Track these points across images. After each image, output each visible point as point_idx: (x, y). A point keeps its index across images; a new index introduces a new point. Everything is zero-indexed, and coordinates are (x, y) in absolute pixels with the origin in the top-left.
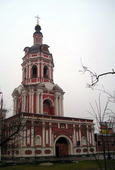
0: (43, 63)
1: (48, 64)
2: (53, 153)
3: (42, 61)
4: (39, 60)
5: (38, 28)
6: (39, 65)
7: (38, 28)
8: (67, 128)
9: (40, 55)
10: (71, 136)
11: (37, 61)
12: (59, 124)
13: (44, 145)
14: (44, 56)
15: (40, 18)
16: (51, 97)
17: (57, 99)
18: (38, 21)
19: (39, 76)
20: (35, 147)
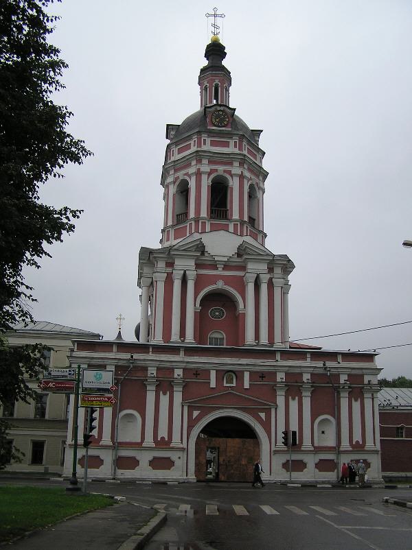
0: (205, 168)
1: (225, 171)
2: (183, 469)
3: (205, 161)
4: (194, 163)
5: (215, 51)
6: (194, 178)
7: (215, 51)
8: (247, 385)
9: (199, 145)
10: (263, 415)
11: (189, 165)
12: (213, 374)
13: (149, 441)
14: (213, 144)
15: (222, 16)
16: (227, 280)
17: (250, 288)
18: (214, 26)
19: (192, 215)
20: (116, 445)
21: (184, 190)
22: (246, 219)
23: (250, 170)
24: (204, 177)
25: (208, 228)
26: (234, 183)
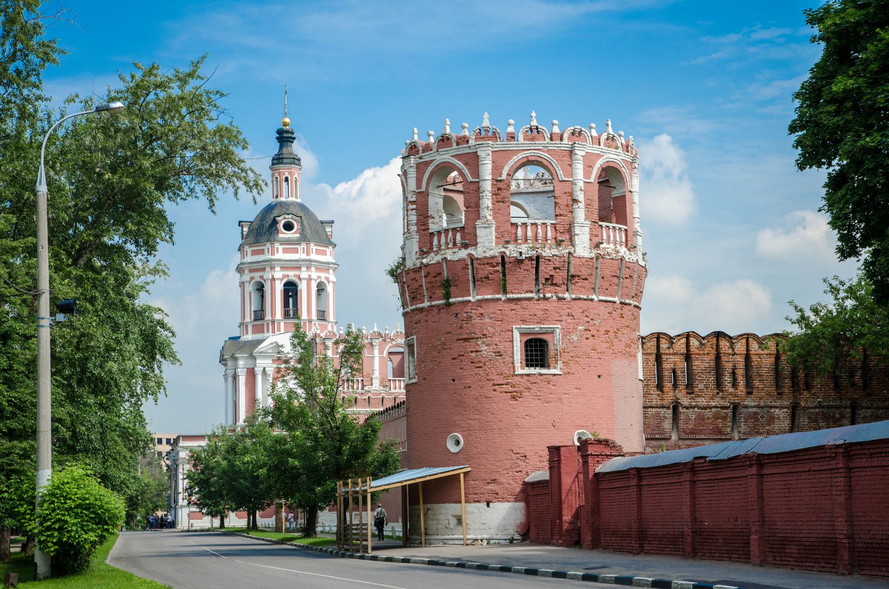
0: (278, 273)
1: (295, 276)
3: (277, 269)
4: (268, 269)
11: (263, 269)
14: (285, 251)
19: (268, 317)
21: (260, 288)
22: (314, 316)
23: (318, 269)
24: (277, 282)
25: (282, 330)
26: (302, 287)
